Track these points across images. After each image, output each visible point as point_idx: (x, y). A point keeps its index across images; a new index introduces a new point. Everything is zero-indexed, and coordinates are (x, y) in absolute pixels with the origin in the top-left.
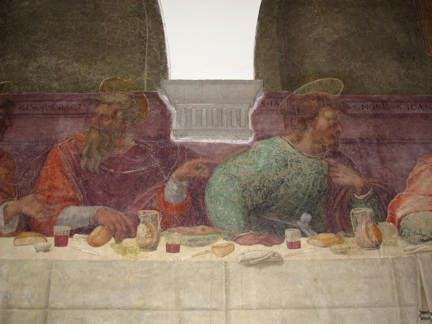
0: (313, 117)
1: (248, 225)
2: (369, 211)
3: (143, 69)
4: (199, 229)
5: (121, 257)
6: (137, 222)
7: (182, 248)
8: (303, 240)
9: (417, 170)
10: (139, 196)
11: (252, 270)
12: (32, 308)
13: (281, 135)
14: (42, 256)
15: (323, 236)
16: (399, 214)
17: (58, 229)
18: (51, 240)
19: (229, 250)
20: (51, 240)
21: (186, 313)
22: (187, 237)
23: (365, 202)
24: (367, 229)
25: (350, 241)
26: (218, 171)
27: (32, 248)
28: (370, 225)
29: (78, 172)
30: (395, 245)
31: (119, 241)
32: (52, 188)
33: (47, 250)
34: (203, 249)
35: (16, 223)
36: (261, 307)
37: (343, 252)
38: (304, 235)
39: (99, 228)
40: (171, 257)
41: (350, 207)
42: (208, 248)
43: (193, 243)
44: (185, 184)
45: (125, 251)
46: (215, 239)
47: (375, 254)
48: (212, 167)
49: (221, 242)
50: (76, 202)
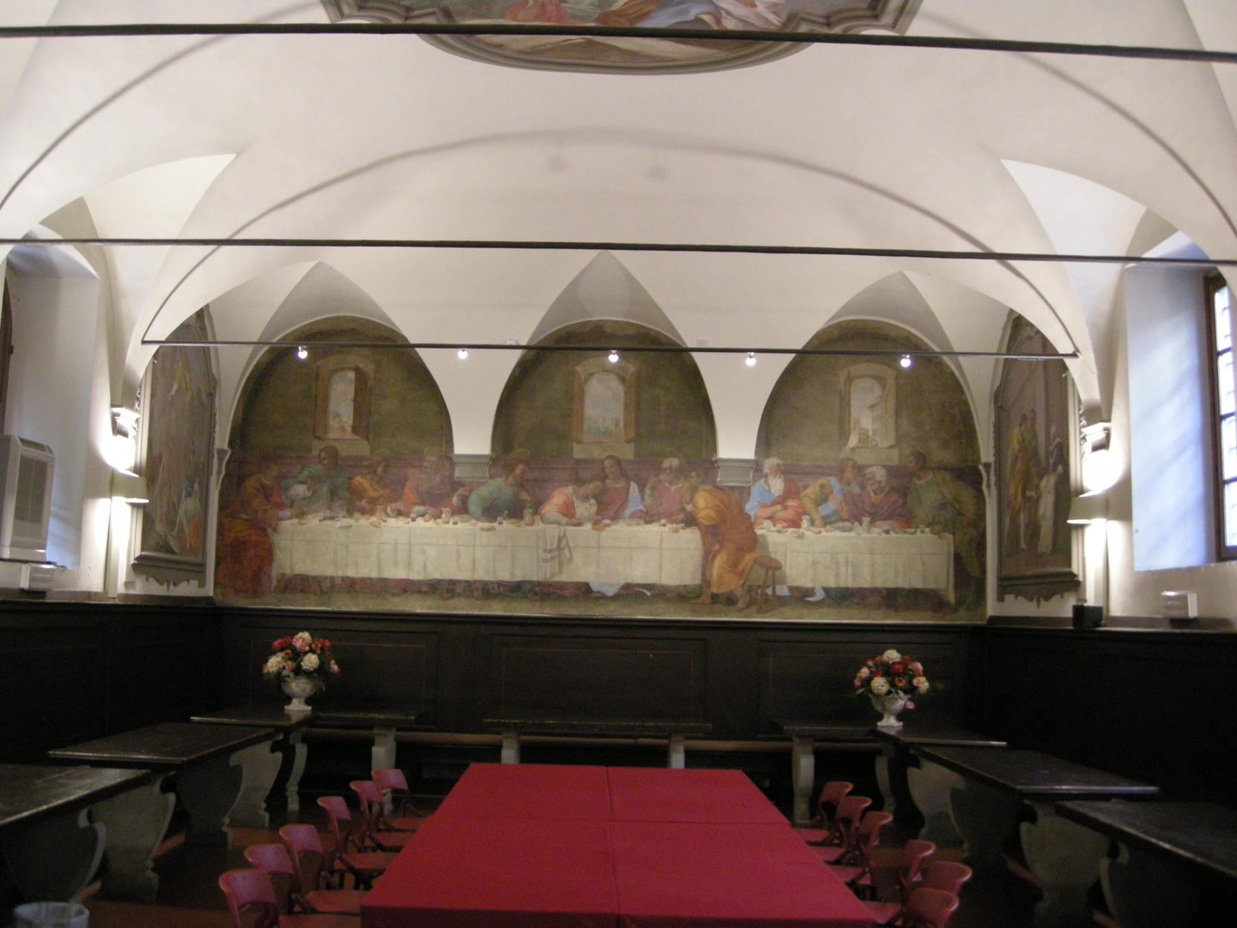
0: (514, 469)
1: (484, 515)
2: (531, 511)
3: (442, 444)
4: (465, 516)
5: (435, 526)
6: (441, 513)
7: (459, 524)
8: (504, 522)
9: (554, 494)
10: (442, 503)
11: (484, 533)
12: (405, 544)
13: (500, 476)
14: (407, 525)
15: (512, 520)
16: (543, 512)
17: (413, 515)
18: (410, 519)
19: (476, 525)
20: (410, 519)
21: (460, 547)
22: (461, 519)
23: (529, 507)
24: (529, 518)
25: (522, 523)
26: (473, 493)
27: (403, 522)
28: (531, 517)
29: (417, 491)
30: (538, 524)
31: (435, 520)
32: (408, 499)
33: (408, 523)
34: (465, 524)
35: (396, 512)
36: (486, 546)
37: (519, 527)
38: (504, 519)
39: (427, 515)
40: (455, 526)
41: (524, 509)
42: (468, 523)
43: (463, 521)
44: (460, 498)
45: (437, 524)
46: (471, 520)
47: (530, 528)
48: (471, 491)
49: (473, 521)
50: (417, 504)
